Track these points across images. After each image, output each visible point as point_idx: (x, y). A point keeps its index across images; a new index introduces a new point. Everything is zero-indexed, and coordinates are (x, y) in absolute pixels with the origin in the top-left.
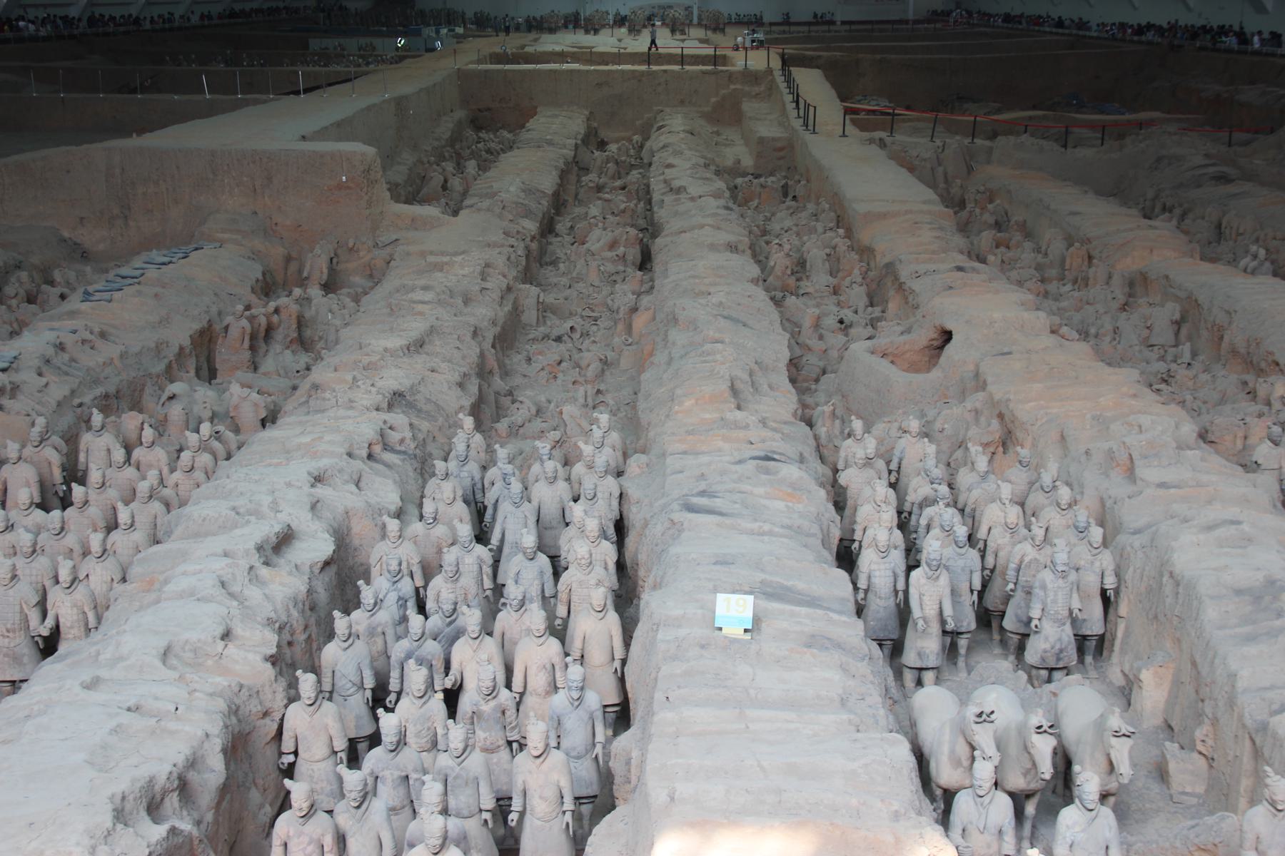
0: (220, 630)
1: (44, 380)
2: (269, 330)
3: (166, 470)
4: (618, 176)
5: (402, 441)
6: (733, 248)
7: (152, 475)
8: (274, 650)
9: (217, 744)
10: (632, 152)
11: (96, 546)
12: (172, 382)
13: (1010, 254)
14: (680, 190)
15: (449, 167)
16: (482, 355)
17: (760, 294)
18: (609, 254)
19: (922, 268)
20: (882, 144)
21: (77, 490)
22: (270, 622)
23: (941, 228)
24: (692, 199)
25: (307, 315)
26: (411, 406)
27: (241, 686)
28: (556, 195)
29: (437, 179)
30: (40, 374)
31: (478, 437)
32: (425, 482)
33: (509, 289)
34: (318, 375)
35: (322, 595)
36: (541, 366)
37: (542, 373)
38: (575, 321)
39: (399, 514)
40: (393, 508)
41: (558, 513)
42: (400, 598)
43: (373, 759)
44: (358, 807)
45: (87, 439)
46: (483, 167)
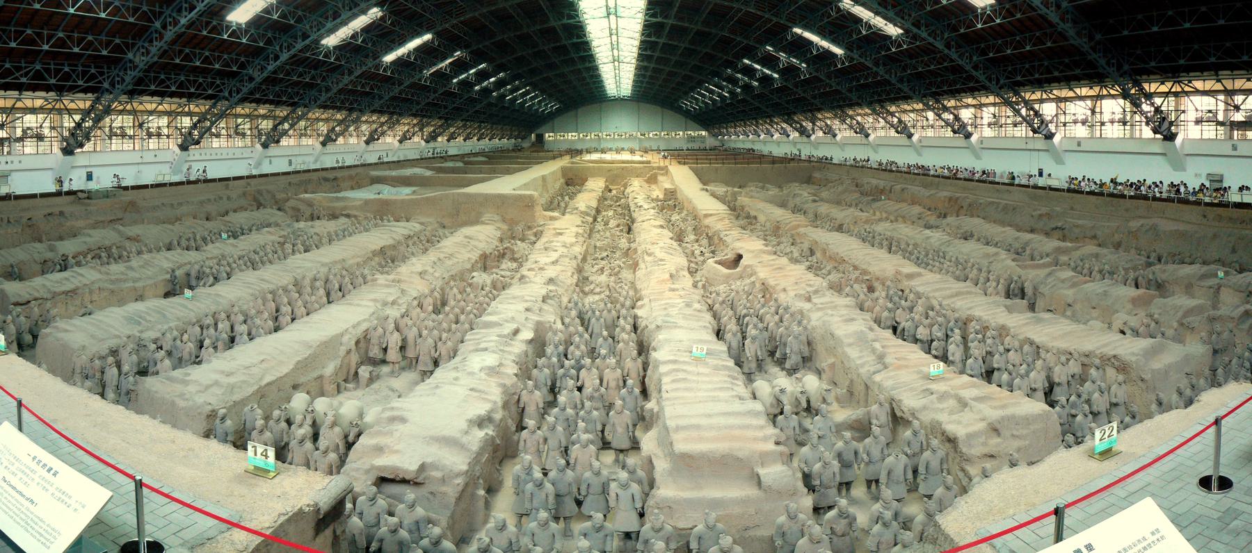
4: (617, 201)
6: (662, 227)
14: (641, 207)
15: (559, 198)
16: (578, 265)
20: (707, 190)
28: (597, 208)
34: (524, 271)
41: (611, 322)
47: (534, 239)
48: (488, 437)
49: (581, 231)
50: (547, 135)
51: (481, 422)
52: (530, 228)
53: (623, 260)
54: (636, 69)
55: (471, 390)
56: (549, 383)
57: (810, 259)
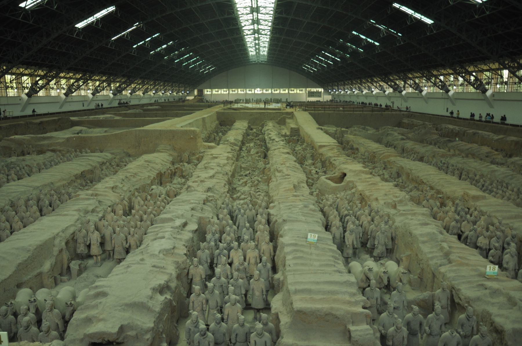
6: (288, 153)
13: (356, 155)
14: (273, 140)
17: (297, 165)
19: (336, 158)
23: (339, 149)
24: (277, 142)
25: (184, 169)
33: (233, 163)
47: (196, 161)
48: (167, 300)
49: (230, 155)
51: (162, 290)
52: (194, 154)
53: (261, 176)
54: (271, 40)
55: (154, 266)
56: (209, 261)
57: (397, 180)
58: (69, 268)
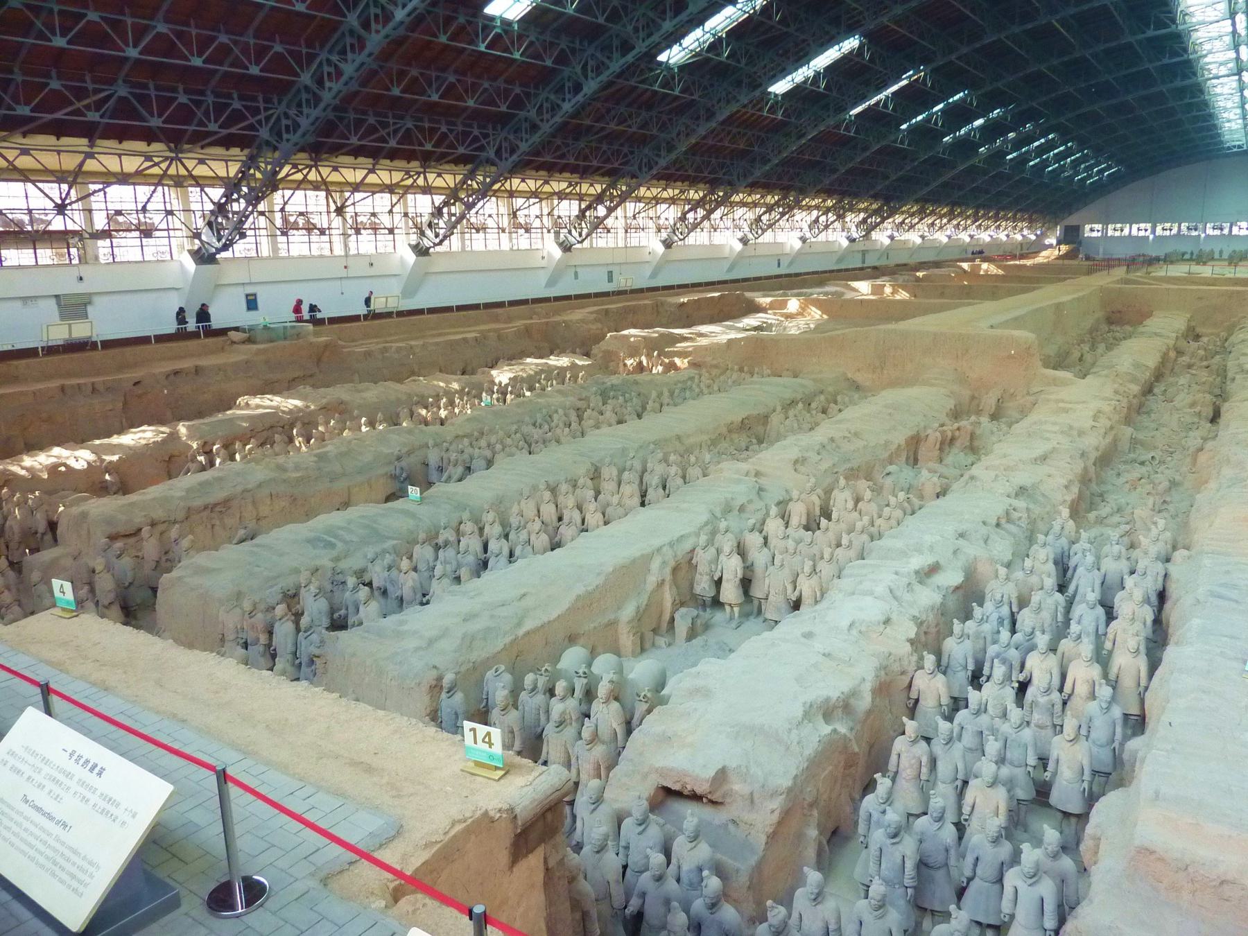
0: (883, 618)
1: (820, 457)
2: (953, 440)
3: (875, 516)
5: (1020, 518)
7: (866, 519)
8: (912, 635)
9: (867, 689)
10: (1219, 343)
11: (827, 556)
12: (891, 464)
15: (1086, 348)
16: (1085, 469)
18: (1189, 410)
21: (824, 522)
22: (914, 618)
25: (978, 432)
26: (1029, 496)
27: (890, 654)
29: (1076, 354)
30: (818, 454)
31: (1071, 522)
32: (1031, 545)
33: (1112, 428)
34: (975, 471)
35: (952, 603)
36: (1125, 480)
37: (1127, 486)
38: (1157, 454)
39: (1008, 565)
40: (1006, 560)
42: (1000, 618)
43: (962, 715)
44: (947, 744)
45: (835, 493)
46: (1109, 348)
47: (1015, 414)
50: (1087, 227)
58: (672, 620)
